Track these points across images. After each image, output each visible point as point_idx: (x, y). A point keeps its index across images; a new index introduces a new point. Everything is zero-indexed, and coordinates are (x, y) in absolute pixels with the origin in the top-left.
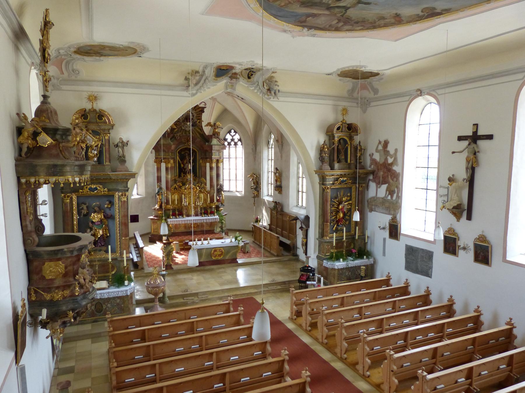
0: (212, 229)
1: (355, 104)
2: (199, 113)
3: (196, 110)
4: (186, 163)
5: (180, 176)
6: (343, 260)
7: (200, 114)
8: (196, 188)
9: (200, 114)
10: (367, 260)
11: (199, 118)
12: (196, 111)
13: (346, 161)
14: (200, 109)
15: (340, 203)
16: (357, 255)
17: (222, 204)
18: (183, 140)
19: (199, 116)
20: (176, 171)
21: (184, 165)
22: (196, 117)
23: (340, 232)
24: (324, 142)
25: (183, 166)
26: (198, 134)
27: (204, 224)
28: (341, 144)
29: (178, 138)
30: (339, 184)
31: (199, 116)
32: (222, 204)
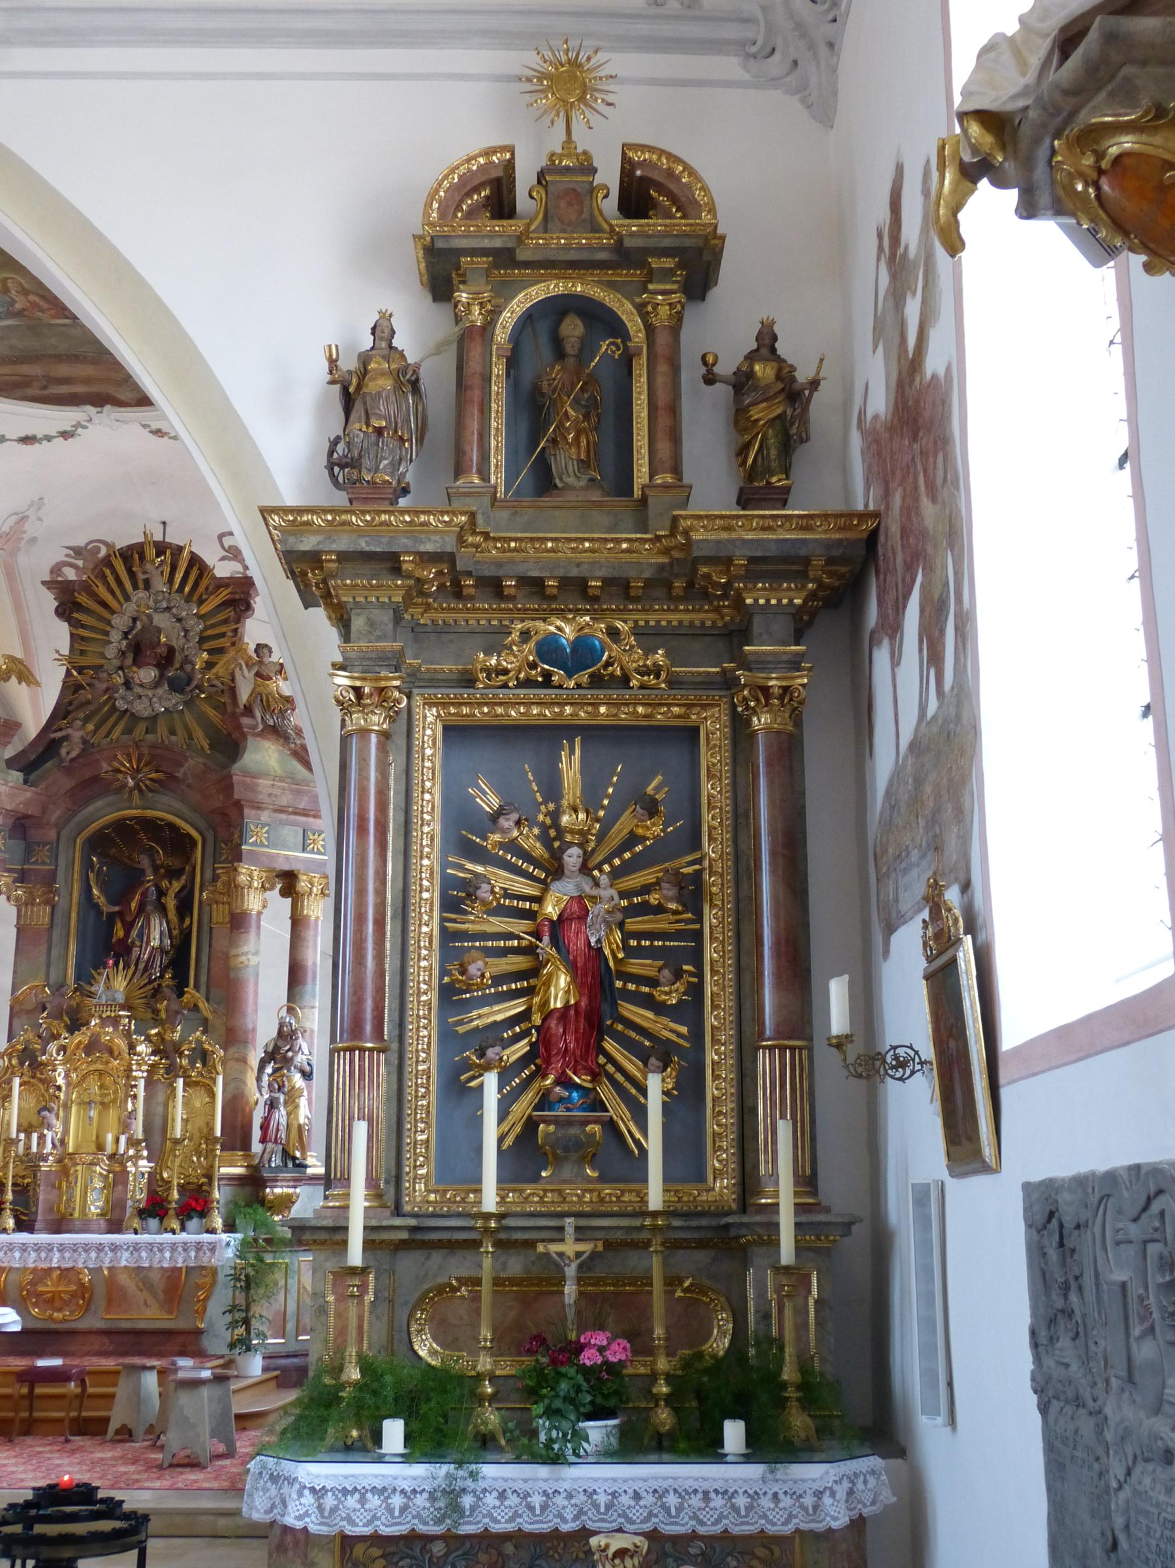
0: (181, 1324)
1: (730, 66)
2: (221, 617)
3: (201, 602)
4: (141, 908)
5: (84, 977)
6: (408, 1438)
7: (226, 621)
8: (132, 1047)
9: (226, 621)
10: (755, 1471)
11: (220, 642)
12: (205, 609)
13: (622, 483)
14: (224, 594)
15: (556, 871)
16: (664, 1417)
17: (286, 1155)
18: (105, 766)
19: (223, 635)
20: (54, 952)
21: (128, 927)
22: (203, 640)
23: (567, 1171)
24: (374, 331)
25: (121, 934)
26: (199, 733)
27: (123, 1279)
28: (571, 348)
29: (73, 754)
30: (528, 683)
31: (223, 635)
32: (286, 1155)
